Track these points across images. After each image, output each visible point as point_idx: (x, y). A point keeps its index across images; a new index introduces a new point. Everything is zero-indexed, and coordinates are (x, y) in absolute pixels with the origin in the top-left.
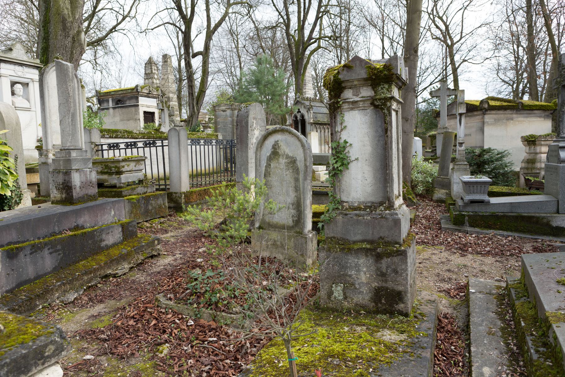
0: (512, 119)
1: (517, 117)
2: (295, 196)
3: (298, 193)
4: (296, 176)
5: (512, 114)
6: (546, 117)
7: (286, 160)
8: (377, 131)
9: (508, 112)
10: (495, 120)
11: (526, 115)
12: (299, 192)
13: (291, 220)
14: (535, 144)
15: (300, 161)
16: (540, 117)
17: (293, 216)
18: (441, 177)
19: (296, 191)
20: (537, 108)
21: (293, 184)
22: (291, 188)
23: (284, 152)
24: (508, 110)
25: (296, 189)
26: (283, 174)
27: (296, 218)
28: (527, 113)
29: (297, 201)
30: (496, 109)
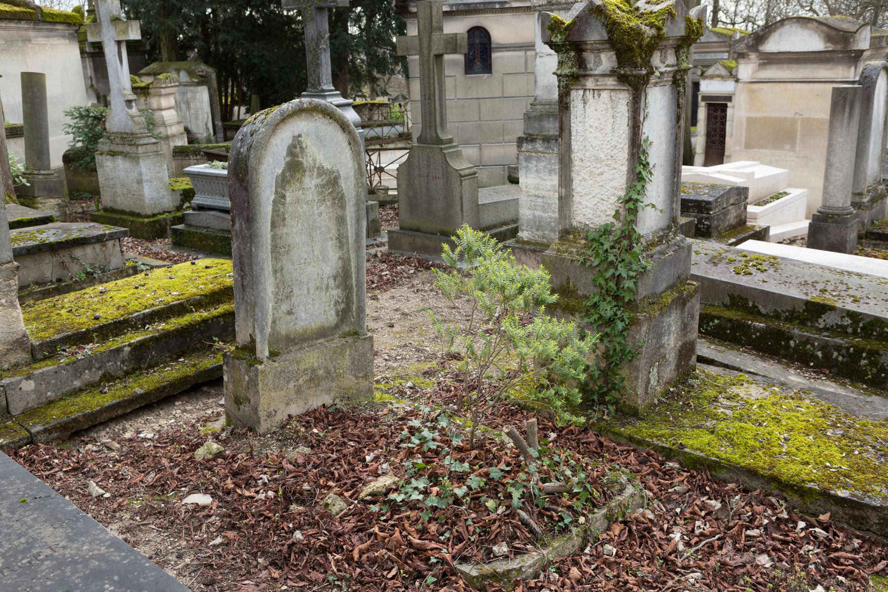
0: (30, 41)
1: (35, 37)
2: (340, 258)
3: (345, 250)
4: (340, 213)
5: (27, 29)
6: (71, 37)
7: (319, 181)
8: (671, 121)
9: (23, 25)
10: (7, 41)
11: (46, 33)
12: (345, 247)
13: (333, 312)
14: (148, 94)
15: (346, 179)
16: (64, 37)
17: (337, 303)
18: (42, 172)
19: (340, 247)
20: (62, 20)
21: (334, 233)
22: (330, 243)
23: (314, 160)
24: (23, 22)
25: (340, 242)
26: (313, 213)
27: (343, 306)
28: (47, 29)
29: (344, 267)
30: (6, 19)
